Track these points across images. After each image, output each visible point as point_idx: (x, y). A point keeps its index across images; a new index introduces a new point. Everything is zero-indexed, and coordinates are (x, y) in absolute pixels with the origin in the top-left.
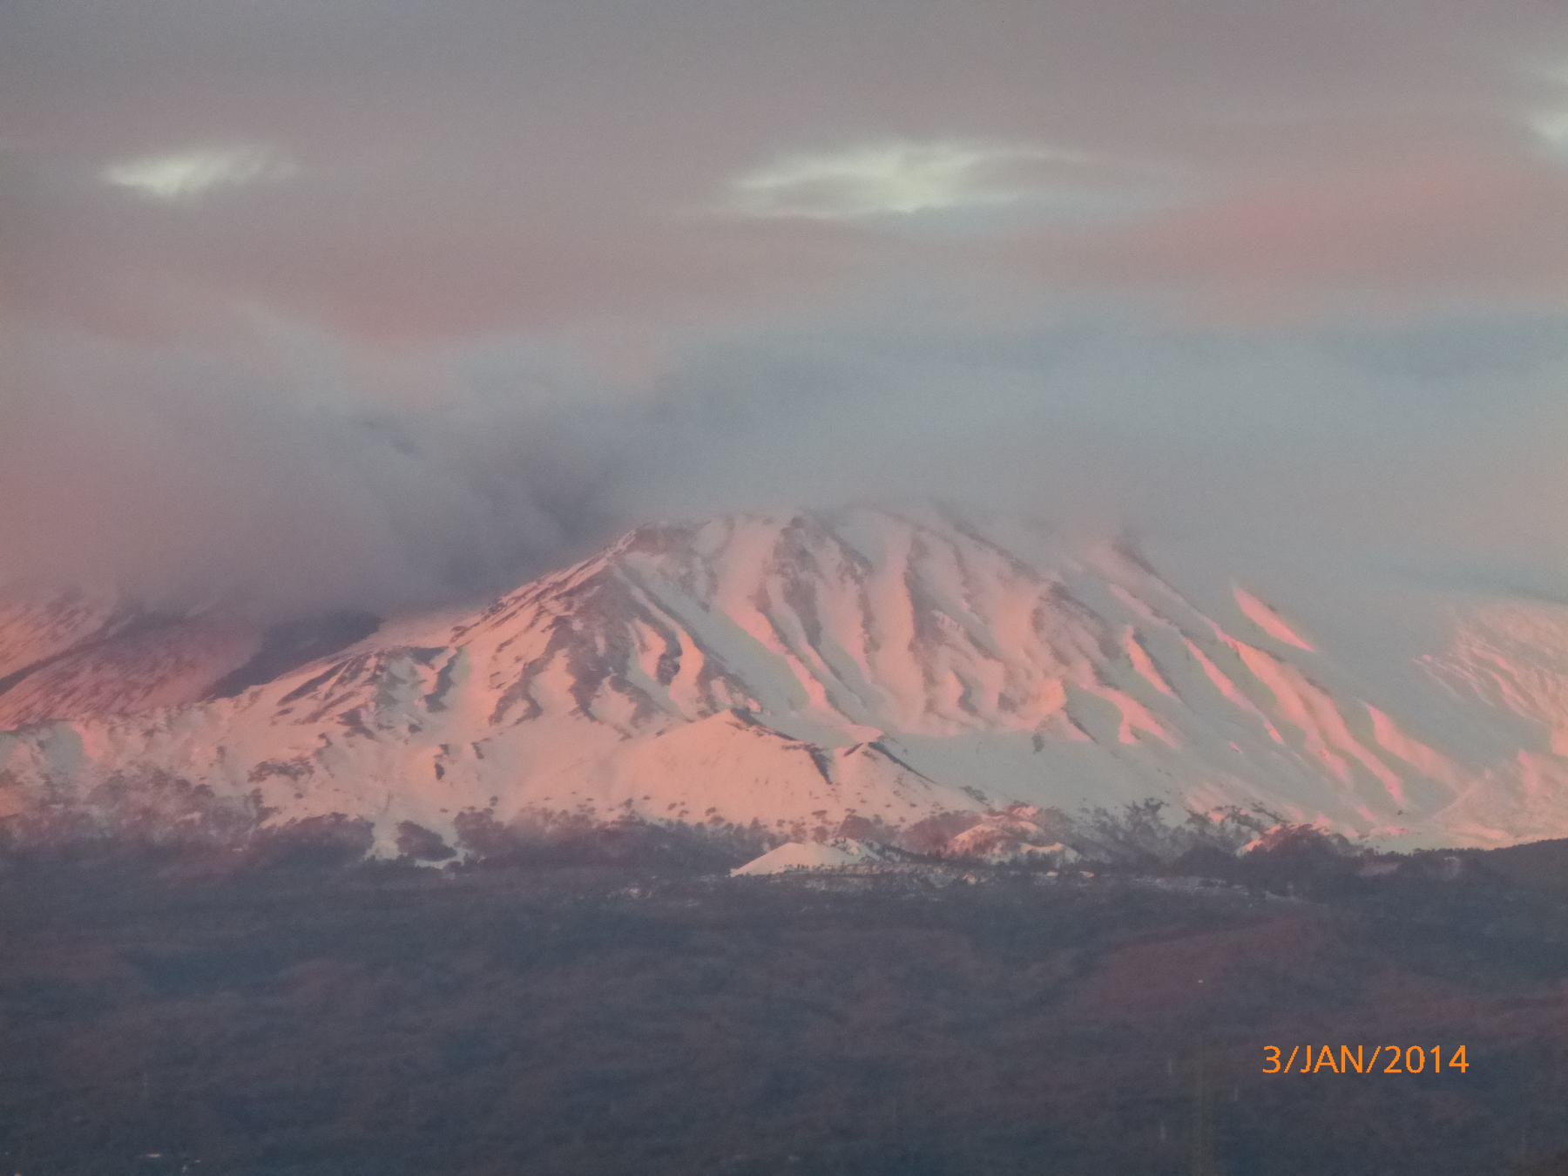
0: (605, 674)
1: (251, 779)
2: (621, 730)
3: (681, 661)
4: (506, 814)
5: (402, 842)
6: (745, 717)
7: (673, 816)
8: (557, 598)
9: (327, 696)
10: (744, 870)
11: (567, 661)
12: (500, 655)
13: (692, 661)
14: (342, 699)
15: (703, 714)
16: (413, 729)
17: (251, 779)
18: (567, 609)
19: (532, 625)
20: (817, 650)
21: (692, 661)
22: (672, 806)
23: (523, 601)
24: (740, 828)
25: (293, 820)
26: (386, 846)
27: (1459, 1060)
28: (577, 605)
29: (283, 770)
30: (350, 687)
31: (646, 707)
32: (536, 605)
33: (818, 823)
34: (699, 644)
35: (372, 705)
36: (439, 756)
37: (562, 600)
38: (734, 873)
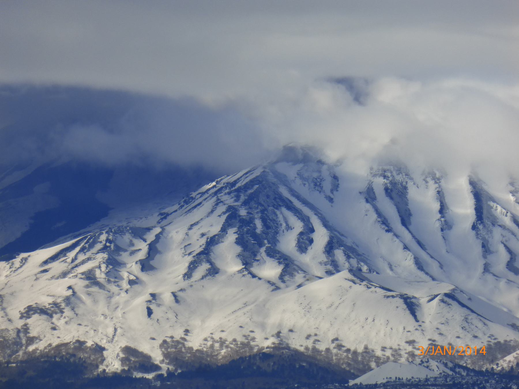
0: (261, 245)
1: (21, 318)
2: (273, 284)
3: (315, 236)
4: (195, 342)
5: (123, 361)
6: (357, 275)
7: (310, 344)
8: (229, 193)
9: (73, 261)
10: (358, 381)
11: (236, 236)
12: (191, 232)
13: (321, 237)
14: (83, 262)
15: (329, 273)
16: (131, 283)
17: (21, 318)
18: (236, 201)
19: (212, 211)
20: (408, 229)
21: (321, 237)
22: (308, 337)
23: (206, 196)
24: (355, 353)
25: (50, 345)
26: (113, 364)
27: (483, 351)
28: (243, 198)
29: (43, 311)
30: (88, 254)
31: (289, 267)
32: (215, 199)
33: (410, 348)
34: (326, 224)
35: (103, 267)
36: (150, 301)
37: (232, 195)
38: (351, 383)
